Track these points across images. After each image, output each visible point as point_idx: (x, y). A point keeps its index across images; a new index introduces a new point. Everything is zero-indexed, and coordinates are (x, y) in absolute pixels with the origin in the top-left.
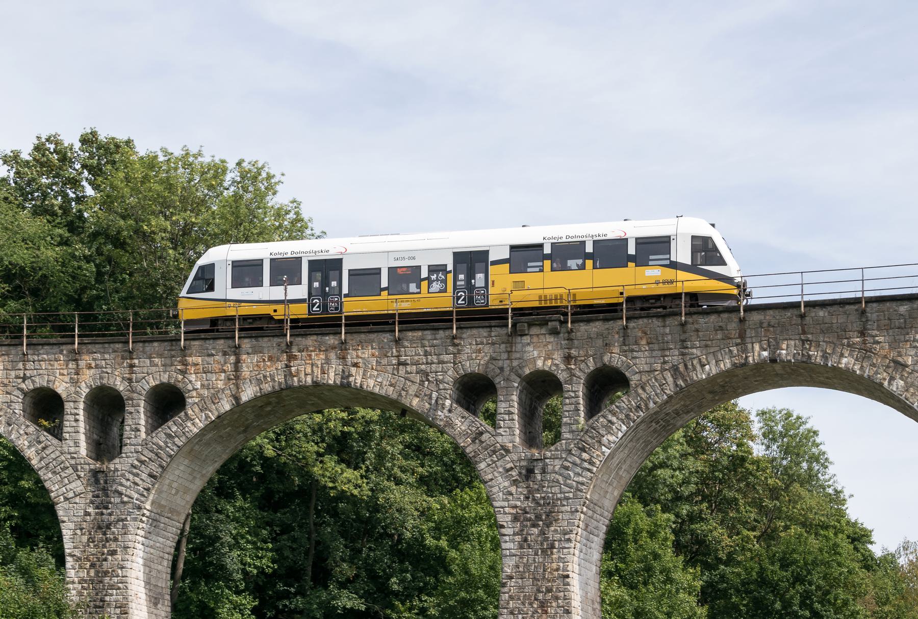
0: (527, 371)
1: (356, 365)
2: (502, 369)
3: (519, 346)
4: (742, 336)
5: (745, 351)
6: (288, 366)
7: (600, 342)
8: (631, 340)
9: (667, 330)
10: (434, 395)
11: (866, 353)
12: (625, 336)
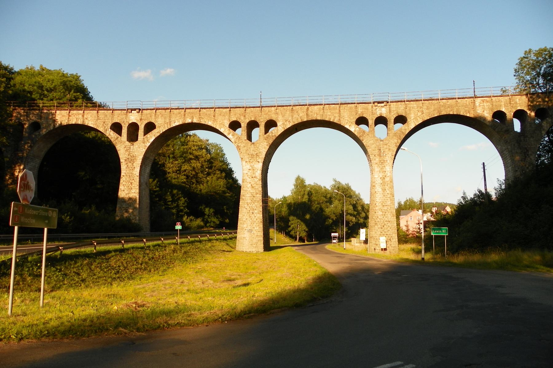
0: (130, 122)
1: (86, 119)
2: (124, 121)
3: (129, 116)
4: (185, 115)
5: (185, 119)
6: (69, 118)
7: (149, 116)
8: (157, 115)
9: (166, 113)
10: (106, 127)
11: (215, 120)
12: (155, 114)
